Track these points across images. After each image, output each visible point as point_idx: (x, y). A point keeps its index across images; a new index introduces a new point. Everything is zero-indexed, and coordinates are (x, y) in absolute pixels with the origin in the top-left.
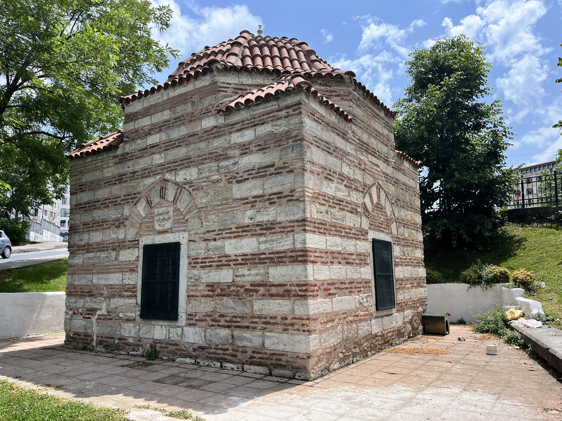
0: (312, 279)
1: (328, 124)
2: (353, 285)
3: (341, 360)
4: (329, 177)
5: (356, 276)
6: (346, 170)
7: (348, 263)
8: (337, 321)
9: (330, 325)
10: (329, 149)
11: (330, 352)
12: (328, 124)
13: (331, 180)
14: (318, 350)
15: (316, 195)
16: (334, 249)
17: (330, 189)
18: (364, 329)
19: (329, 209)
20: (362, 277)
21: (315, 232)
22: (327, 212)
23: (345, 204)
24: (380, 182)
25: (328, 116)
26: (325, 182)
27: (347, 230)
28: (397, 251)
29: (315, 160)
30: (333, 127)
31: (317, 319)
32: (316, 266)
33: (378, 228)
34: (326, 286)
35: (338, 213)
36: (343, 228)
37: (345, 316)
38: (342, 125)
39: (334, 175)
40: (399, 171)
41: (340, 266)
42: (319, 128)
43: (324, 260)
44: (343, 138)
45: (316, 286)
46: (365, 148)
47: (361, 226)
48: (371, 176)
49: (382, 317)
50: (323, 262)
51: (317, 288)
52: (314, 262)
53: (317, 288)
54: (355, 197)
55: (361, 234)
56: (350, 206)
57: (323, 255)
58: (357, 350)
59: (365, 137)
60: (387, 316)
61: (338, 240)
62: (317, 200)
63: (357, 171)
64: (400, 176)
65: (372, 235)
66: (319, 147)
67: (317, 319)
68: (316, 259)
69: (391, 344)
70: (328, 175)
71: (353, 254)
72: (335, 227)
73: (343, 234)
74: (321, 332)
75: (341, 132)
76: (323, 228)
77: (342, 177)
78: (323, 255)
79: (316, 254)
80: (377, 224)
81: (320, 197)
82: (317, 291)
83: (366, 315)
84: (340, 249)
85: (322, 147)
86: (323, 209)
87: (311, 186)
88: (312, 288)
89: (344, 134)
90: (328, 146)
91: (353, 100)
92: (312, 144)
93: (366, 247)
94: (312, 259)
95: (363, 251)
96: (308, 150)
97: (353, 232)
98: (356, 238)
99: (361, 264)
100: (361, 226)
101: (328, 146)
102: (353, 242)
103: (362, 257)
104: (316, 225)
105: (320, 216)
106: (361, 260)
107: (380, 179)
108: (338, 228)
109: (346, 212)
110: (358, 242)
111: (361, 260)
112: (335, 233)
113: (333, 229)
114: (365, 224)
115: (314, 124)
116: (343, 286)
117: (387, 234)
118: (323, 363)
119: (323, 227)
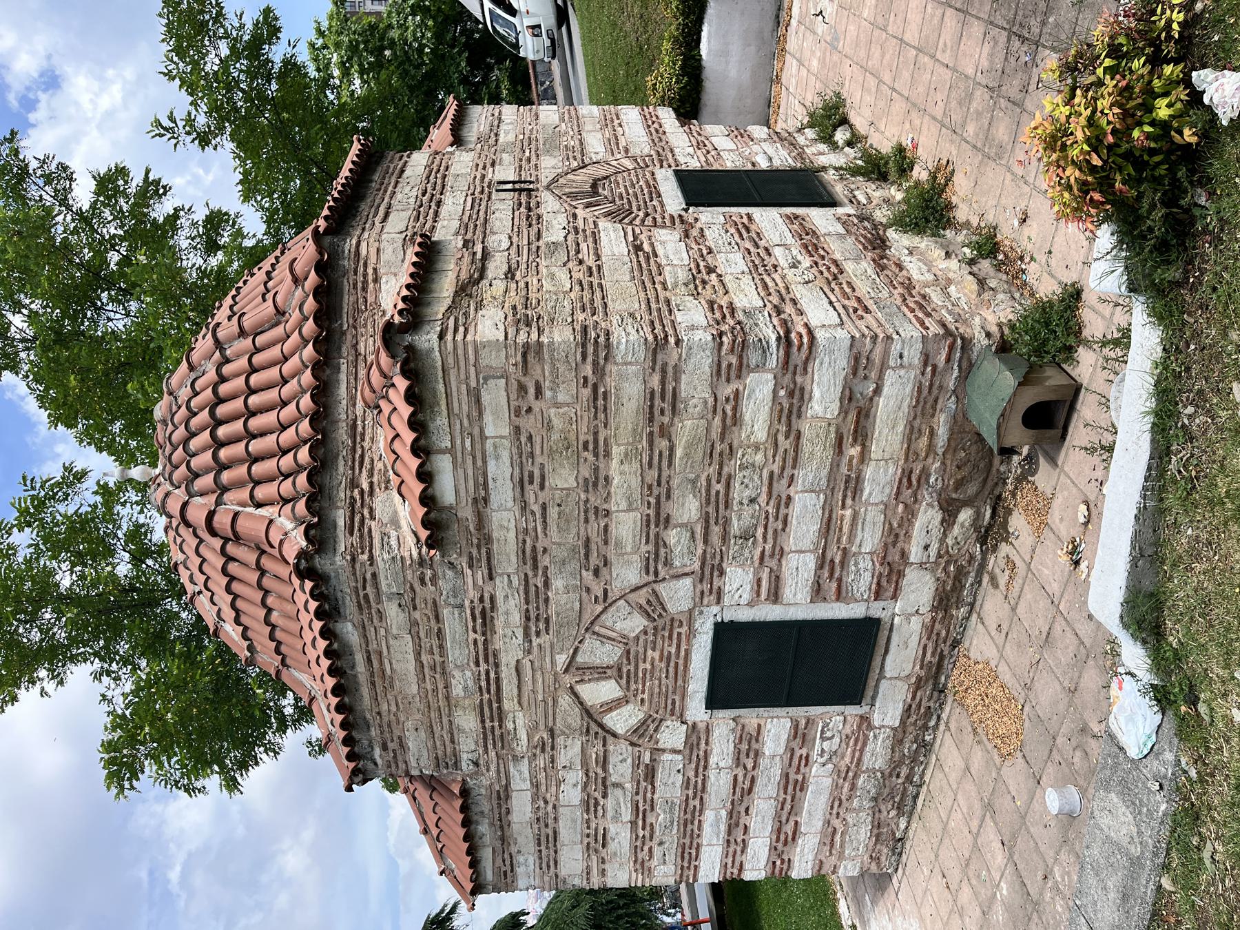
0: (764, 874)
1: (503, 839)
2: (792, 777)
3: (900, 813)
4: (600, 838)
5: (776, 772)
6: (571, 794)
7: (750, 790)
8: (836, 823)
9: (838, 838)
10: (548, 841)
11: (878, 836)
12: (503, 839)
13: (604, 835)
14: (862, 862)
15: (638, 866)
16: (723, 827)
17: (621, 838)
18: (877, 754)
19: (656, 840)
20: (781, 751)
21: (696, 867)
22: (661, 844)
23: (640, 798)
24: (562, 659)
25: (487, 839)
26: (612, 846)
27: (691, 792)
28: (740, 598)
29: (579, 867)
30: (502, 827)
31: (821, 862)
32: (747, 866)
33: (680, 673)
34: (780, 846)
35: (660, 818)
36: (687, 805)
37: (836, 804)
38: (484, 805)
39: (593, 825)
40: (488, 539)
41: (753, 811)
42: (521, 859)
43: (739, 849)
44: (508, 797)
45: (774, 863)
46: (492, 713)
47: (679, 752)
48: (555, 701)
49: (882, 676)
50: (742, 852)
51: (778, 863)
52: (740, 870)
53: (778, 863)
54: (621, 769)
55: (697, 740)
56: (643, 784)
57: (731, 850)
58: (904, 771)
59: (468, 721)
60: (887, 651)
61: (709, 816)
62: (646, 864)
63: (562, 760)
64: (504, 519)
65: (696, 710)
66: (556, 863)
67: (821, 862)
68: (737, 864)
69: (956, 643)
70: (597, 842)
71: (736, 776)
72: (685, 825)
73: (697, 803)
74: (841, 856)
75: (500, 806)
76: (689, 853)
77: (590, 805)
78: (731, 850)
79: (730, 864)
80: (671, 682)
81: (640, 856)
82: (783, 862)
83: (857, 741)
84: (724, 813)
85: (552, 853)
86: (657, 852)
87: (626, 876)
88: (777, 871)
89: (499, 798)
90: (543, 839)
91: (402, 766)
92: (557, 876)
93: (723, 725)
94: (735, 871)
95: (731, 746)
96: (570, 882)
97: (691, 774)
98: (705, 768)
99: (757, 754)
100: (679, 752)
101: (543, 839)
102: (712, 774)
103: (744, 747)
104: (686, 865)
105: (671, 857)
106: (748, 747)
107: (553, 663)
108: (689, 816)
109: (656, 797)
110: (713, 760)
111: (748, 747)
112: (696, 822)
113: (689, 827)
114: (672, 736)
115: (520, 870)
116: (788, 807)
117: (692, 633)
118: (885, 851)
119: (687, 850)
